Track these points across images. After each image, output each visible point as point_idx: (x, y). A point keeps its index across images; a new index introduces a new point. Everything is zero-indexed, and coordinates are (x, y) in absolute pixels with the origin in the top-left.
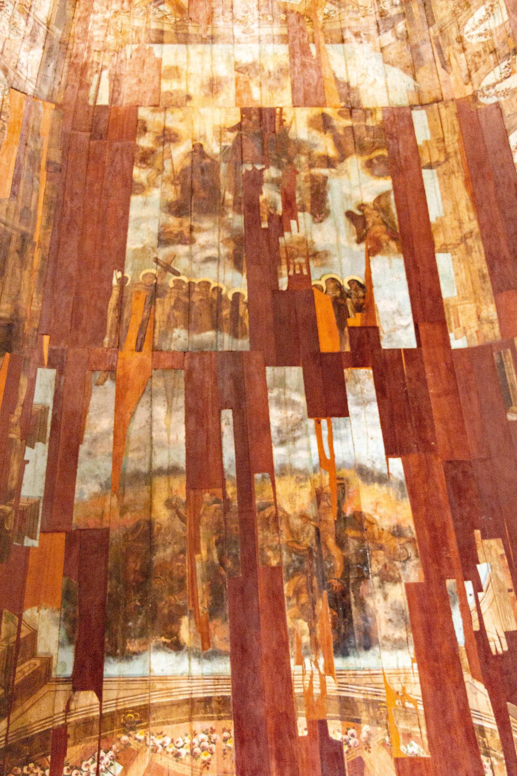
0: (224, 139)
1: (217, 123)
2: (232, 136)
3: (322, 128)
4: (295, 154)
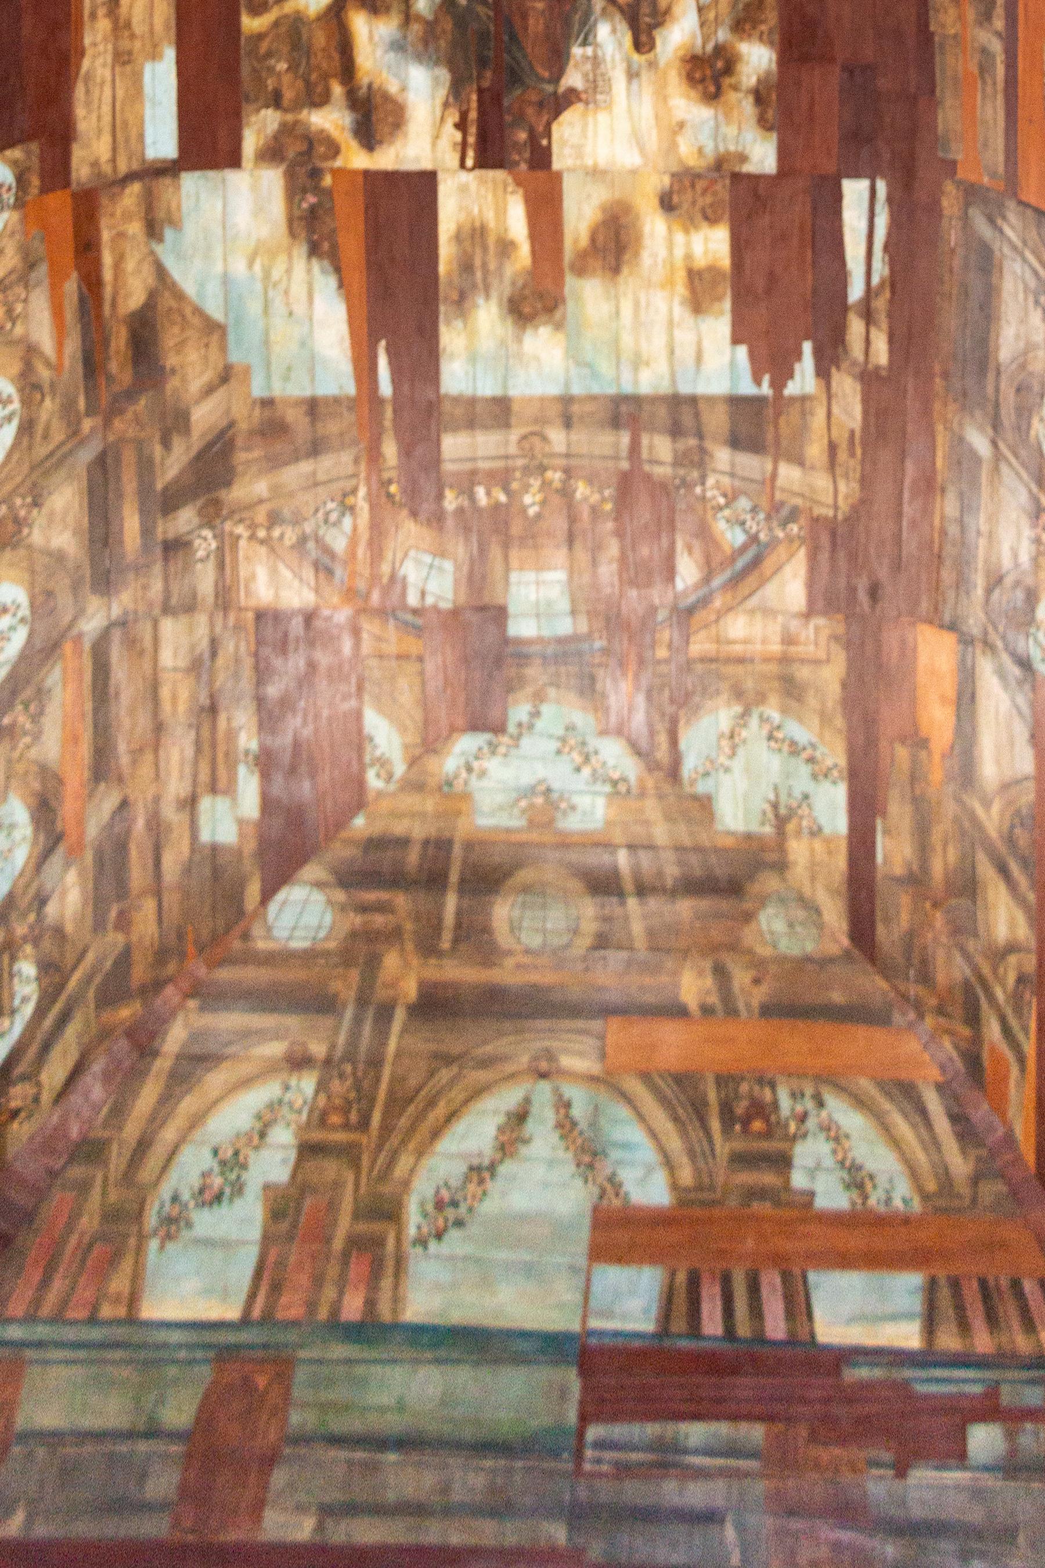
0: (588, 66)
1: (602, 117)
2: (573, 79)
3: (378, 100)
4: (436, 20)
